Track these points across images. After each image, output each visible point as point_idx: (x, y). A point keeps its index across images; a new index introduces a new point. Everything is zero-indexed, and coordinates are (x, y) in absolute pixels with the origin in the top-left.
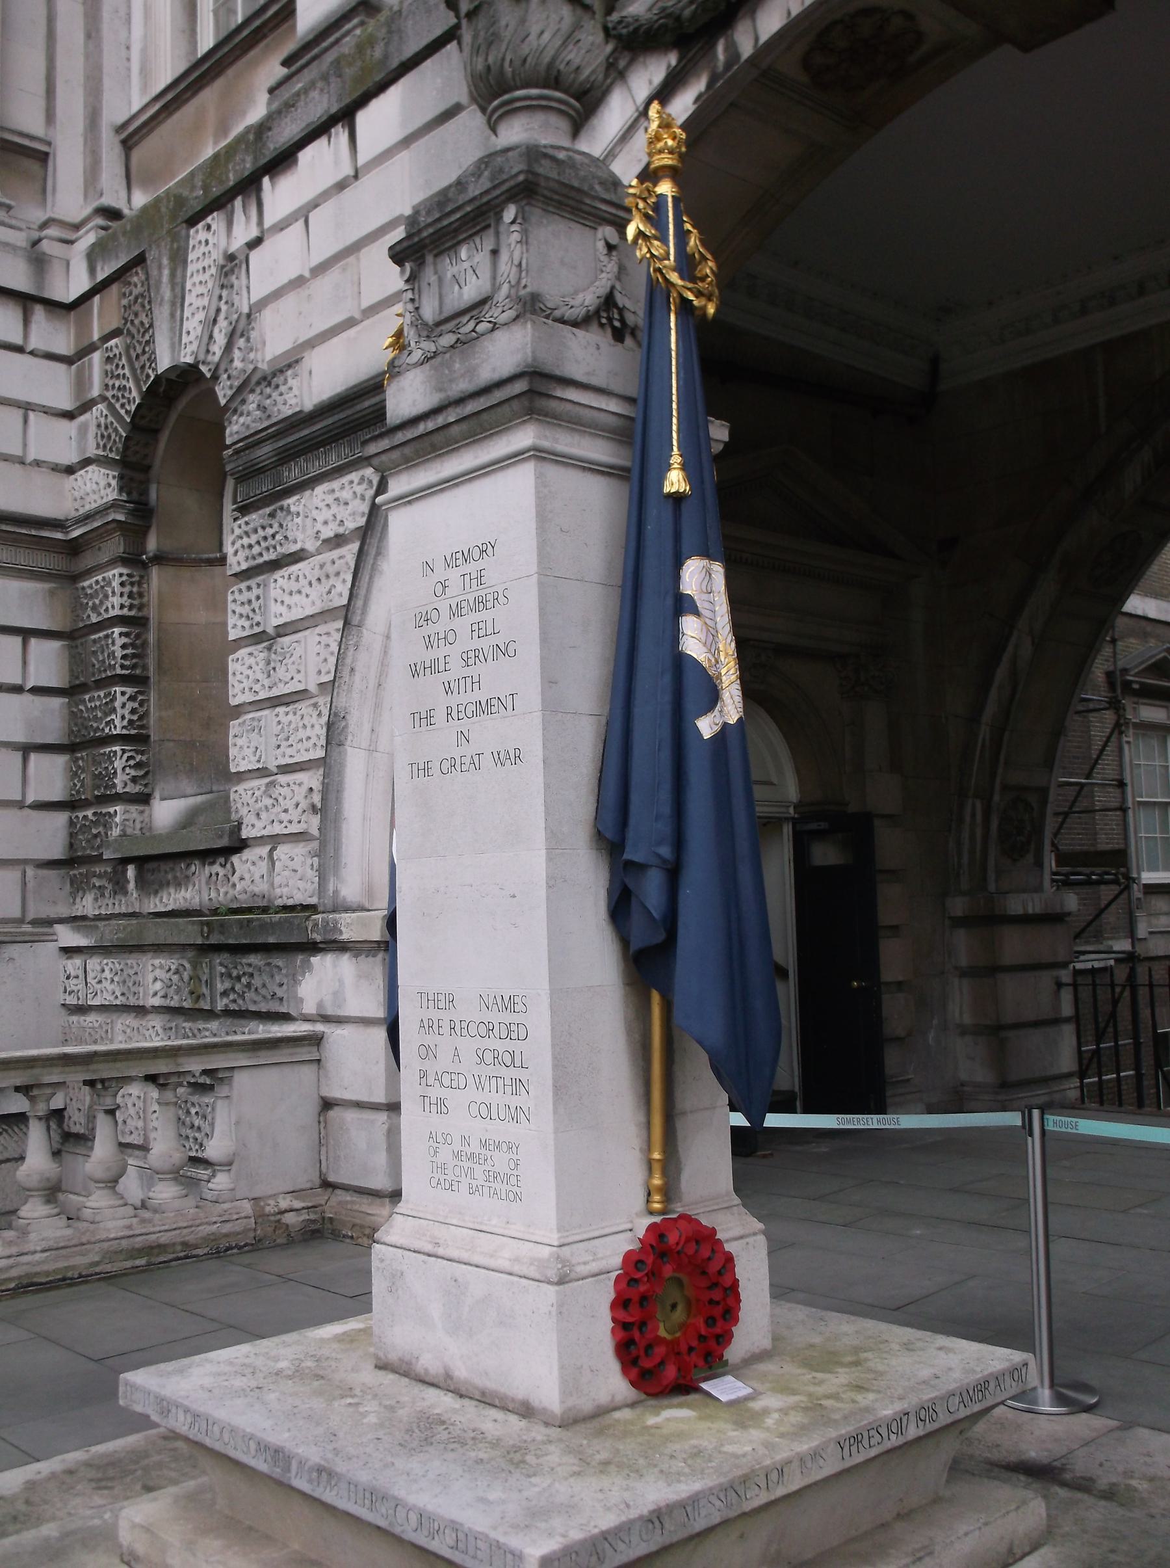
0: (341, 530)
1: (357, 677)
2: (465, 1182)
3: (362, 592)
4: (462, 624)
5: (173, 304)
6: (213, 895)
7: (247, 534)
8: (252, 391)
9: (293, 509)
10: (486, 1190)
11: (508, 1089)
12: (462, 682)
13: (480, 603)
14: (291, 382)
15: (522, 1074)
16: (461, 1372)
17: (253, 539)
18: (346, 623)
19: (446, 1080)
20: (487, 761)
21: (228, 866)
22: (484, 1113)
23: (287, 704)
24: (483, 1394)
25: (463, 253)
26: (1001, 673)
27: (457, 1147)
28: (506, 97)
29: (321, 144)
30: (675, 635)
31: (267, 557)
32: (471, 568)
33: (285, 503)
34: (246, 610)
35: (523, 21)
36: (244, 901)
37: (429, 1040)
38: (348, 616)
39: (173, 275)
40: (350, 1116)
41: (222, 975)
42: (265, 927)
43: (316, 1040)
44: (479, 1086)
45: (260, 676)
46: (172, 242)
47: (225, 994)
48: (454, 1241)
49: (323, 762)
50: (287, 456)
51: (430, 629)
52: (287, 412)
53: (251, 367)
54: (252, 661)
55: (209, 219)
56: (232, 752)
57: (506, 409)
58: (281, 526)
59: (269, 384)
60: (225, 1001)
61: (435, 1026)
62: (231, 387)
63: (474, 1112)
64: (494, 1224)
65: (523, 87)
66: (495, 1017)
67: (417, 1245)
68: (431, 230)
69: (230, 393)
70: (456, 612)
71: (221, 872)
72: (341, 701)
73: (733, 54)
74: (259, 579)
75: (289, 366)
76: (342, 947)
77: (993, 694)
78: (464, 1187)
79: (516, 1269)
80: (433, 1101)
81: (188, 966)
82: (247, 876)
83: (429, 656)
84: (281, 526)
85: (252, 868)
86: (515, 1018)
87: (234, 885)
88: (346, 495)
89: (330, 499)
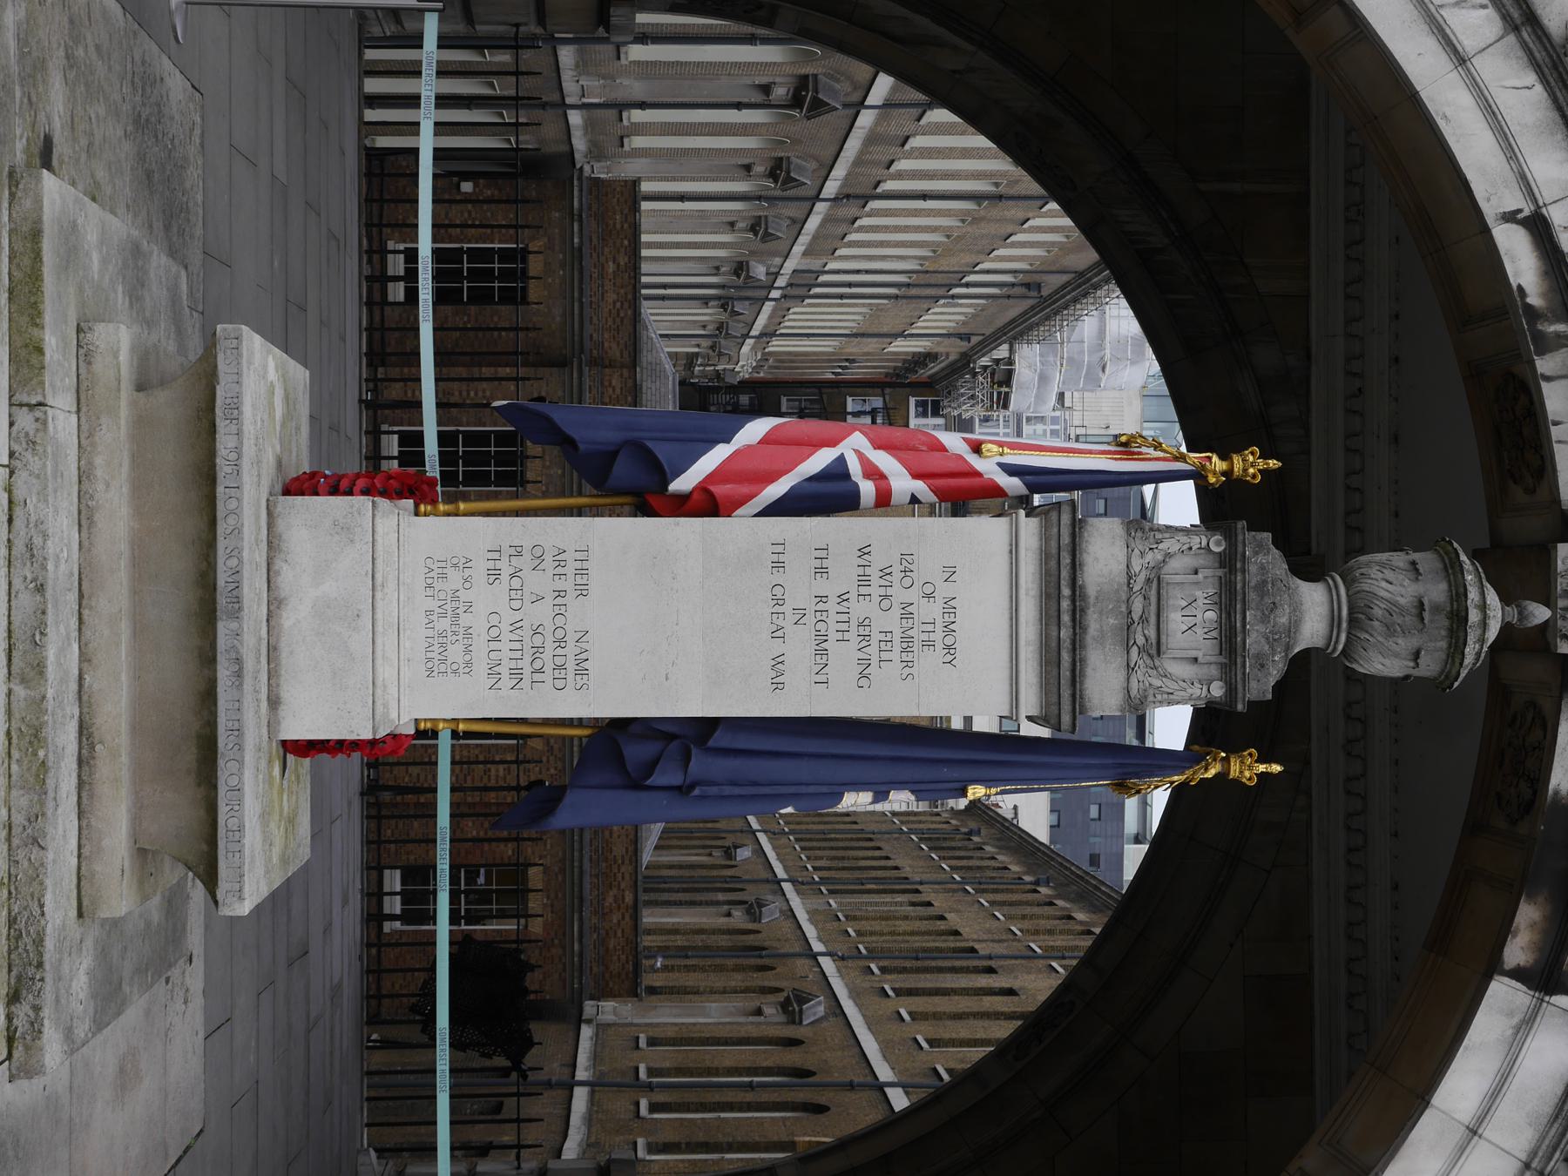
2: (432, 604)
4: (892, 622)
10: (430, 633)
11: (513, 664)
12: (844, 617)
13: (907, 640)
15: (526, 683)
19: (516, 583)
20: (777, 647)
22: (494, 632)
24: (275, 649)
25: (1211, 615)
28: (1344, 625)
30: (857, 786)
32: (938, 636)
35: (1397, 655)
37: (548, 558)
44: (516, 626)
51: (897, 575)
57: (1054, 699)
61: (560, 570)
63: (494, 620)
65: (1348, 638)
66: (571, 649)
67: (379, 562)
68: (1239, 586)
70: (907, 615)
78: (432, 604)
79: (379, 692)
80: (499, 565)
83: (874, 572)
86: (570, 676)
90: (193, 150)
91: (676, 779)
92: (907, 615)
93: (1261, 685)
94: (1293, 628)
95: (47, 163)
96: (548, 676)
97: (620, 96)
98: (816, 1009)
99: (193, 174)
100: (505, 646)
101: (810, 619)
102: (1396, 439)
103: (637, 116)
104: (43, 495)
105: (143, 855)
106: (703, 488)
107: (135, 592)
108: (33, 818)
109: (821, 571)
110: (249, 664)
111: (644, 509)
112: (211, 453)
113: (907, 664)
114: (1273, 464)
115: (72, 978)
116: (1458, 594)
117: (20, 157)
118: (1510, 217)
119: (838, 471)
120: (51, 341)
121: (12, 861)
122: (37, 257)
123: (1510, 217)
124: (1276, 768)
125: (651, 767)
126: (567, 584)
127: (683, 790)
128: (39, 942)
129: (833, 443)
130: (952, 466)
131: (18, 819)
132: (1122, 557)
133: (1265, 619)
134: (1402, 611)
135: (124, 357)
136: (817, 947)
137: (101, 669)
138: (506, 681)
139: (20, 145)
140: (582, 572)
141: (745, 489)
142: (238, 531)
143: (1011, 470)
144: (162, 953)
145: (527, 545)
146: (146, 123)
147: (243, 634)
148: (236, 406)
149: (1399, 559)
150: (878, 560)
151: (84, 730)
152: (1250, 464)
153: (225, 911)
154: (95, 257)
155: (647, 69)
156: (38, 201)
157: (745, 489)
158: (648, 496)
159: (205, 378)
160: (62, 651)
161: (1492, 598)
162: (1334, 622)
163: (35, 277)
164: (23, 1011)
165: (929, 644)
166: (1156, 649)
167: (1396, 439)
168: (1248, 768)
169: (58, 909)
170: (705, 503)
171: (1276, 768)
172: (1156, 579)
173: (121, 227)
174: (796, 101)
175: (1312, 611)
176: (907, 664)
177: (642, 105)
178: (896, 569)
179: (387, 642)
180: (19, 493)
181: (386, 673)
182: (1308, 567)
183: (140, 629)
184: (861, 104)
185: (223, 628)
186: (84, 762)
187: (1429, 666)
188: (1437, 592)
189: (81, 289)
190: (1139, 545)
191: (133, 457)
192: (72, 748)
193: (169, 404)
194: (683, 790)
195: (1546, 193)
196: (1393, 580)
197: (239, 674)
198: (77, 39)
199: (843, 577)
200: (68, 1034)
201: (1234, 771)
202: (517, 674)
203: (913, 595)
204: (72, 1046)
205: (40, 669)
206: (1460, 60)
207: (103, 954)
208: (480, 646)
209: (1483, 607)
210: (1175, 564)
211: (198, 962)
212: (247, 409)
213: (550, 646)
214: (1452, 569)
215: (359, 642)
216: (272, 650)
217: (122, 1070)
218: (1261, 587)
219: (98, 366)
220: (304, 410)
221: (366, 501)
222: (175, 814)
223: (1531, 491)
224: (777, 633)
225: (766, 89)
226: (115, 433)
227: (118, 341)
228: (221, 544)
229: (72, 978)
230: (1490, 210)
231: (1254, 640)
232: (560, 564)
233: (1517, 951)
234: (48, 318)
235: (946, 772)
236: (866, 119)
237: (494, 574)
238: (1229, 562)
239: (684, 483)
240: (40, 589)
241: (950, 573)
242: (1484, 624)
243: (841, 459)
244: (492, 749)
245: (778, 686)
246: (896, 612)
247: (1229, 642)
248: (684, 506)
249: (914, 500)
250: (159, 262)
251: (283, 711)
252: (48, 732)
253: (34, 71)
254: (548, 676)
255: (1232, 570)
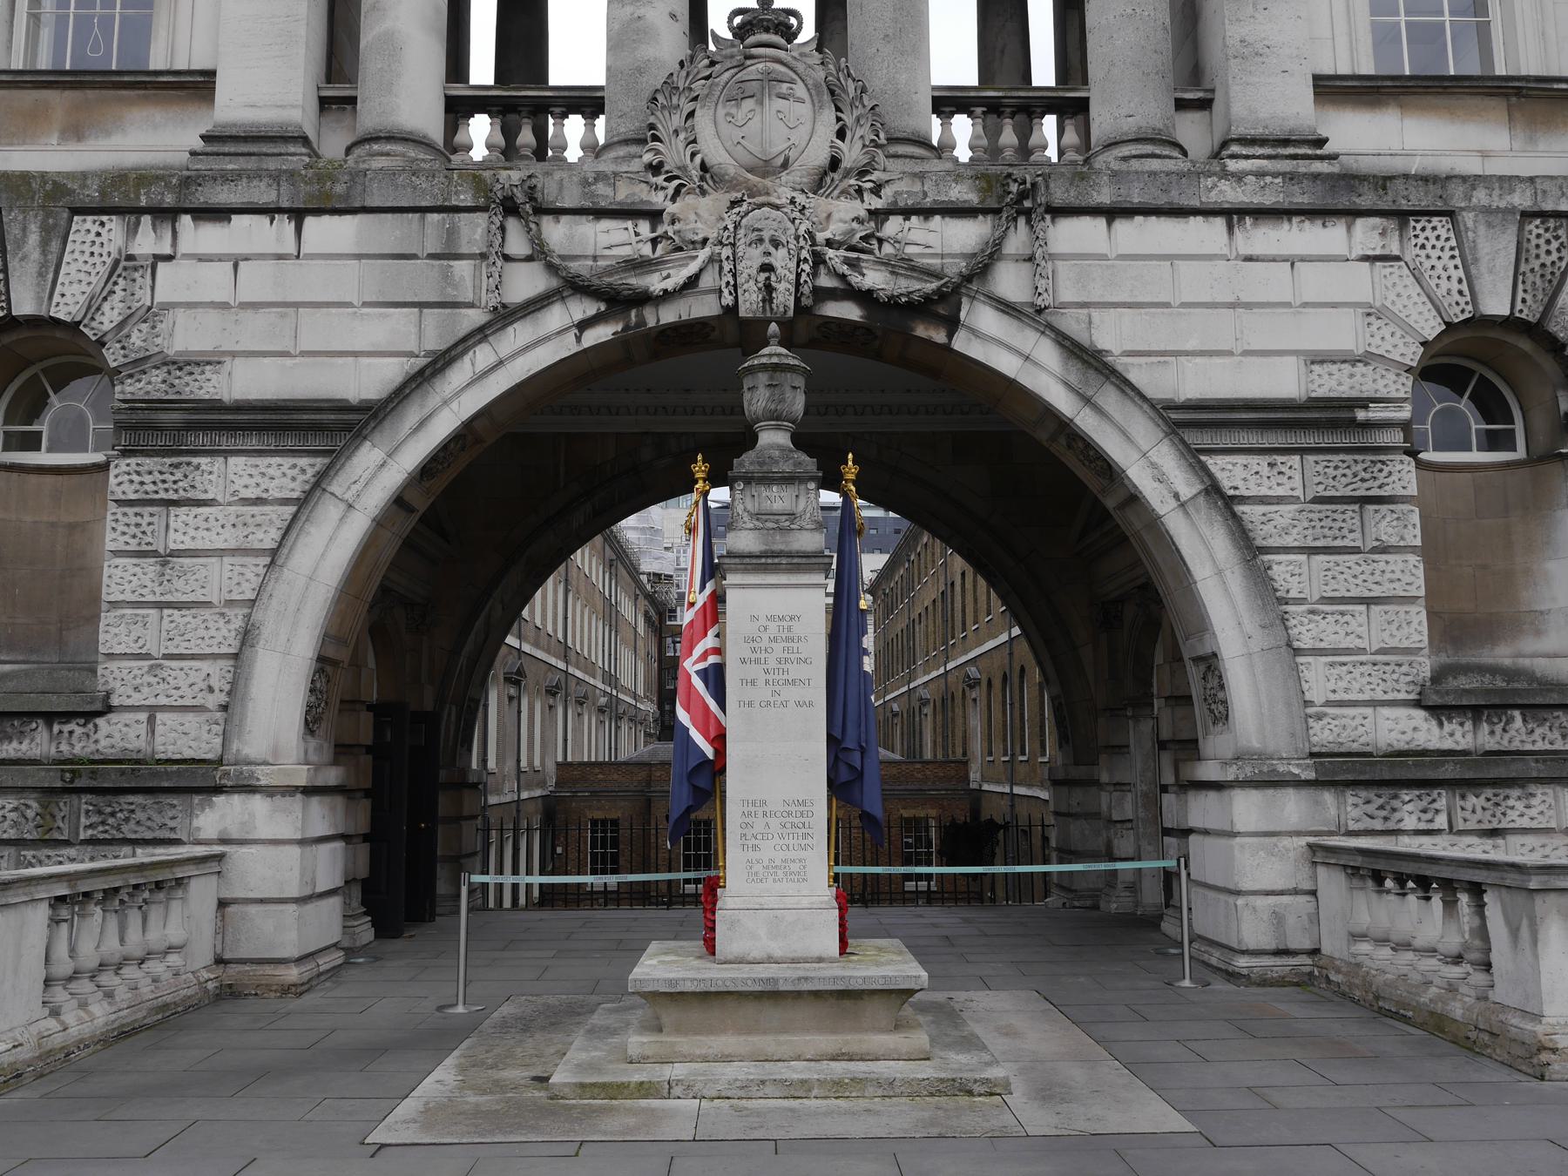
0: (264, 495)
1: (274, 602)
2: (770, 879)
3: (289, 544)
4: (778, 647)
5: (43, 265)
6: (64, 747)
7: (138, 473)
8: (157, 368)
9: (203, 467)
13: (787, 639)
14: (208, 375)
16: (778, 953)
17: (147, 479)
18: (272, 562)
20: (791, 704)
21: (91, 726)
23: (180, 609)
25: (775, 488)
26: (479, 624)
27: (766, 863)
29: (265, 220)
30: (861, 664)
31: (162, 495)
33: (195, 460)
34: (133, 530)
36: (111, 753)
38: (273, 555)
39: (44, 244)
40: (253, 909)
41: (87, 812)
42: (155, 774)
43: (220, 858)
44: (782, 837)
45: (149, 584)
46: (48, 216)
47: (91, 826)
48: (772, 902)
49: (236, 656)
50: (191, 427)
52: (202, 395)
53: (157, 350)
54: (137, 569)
55: (105, 218)
56: (102, 637)
58: (186, 476)
59: (180, 369)
60: (90, 832)
62: (125, 356)
64: (790, 892)
66: (793, 809)
69: (122, 360)
70: (775, 640)
71: (79, 731)
72: (257, 616)
73: (642, 322)
74: (151, 509)
75: (209, 363)
76: (248, 788)
77: (472, 636)
78: (770, 879)
81: (35, 805)
82: (117, 735)
83: (753, 656)
84: (186, 476)
85: (125, 729)
87: (96, 741)
88: (271, 471)
89: (253, 471)
90: (540, 1000)
91: (857, 755)
92: (775, 640)
93: (809, 463)
94: (781, 448)
95: (547, 1079)
96: (806, 820)
97: (514, 773)
98: (973, 671)
99: (552, 1000)
100: (791, 842)
101: (777, 688)
102: (688, 391)
103: (524, 763)
104: (716, 1081)
105: (898, 1027)
106: (711, 742)
107: (765, 1033)
108: (880, 1085)
109: (753, 682)
110: (801, 974)
111: (723, 770)
112: (694, 994)
113: (799, 639)
114: (700, 457)
115: (960, 1062)
116: (764, 368)
117: (543, 1094)
118: (578, 339)
119: (703, 674)
120: (637, 1078)
121: (901, 1095)
122: (593, 1085)
123: (578, 339)
124: (850, 456)
125: (851, 767)
126: (760, 811)
127: (863, 751)
128: (942, 1080)
129: (689, 677)
130: (701, 617)
131: (880, 1092)
132: (745, 533)
133: (777, 462)
134: (773, 394)
135: (645, 1040)
136: (942, 670)
137: (803, 1051)
138: (809, 841)
139: (537, 1094)
140: (754, 804)
141: (712, 721)
142: (733, 980)
143: (703, 587)
144: (947, 1015)
145: (740, 831)
146: (525, 1025)
147: (785, 977)
148: (670, 981)
149: (747, 396)
150: (747, 654)
151: (834, 1058)
152: (700, 468)
153: (926, 985)
154: (594, 1054)
155: (500, 759)
156: (565, 1085)
157: (712, 721)
158: (717, 768)
159: (654, 997)
160: (794, 1070)
161: (766, 351)
162: (778, 428)
163: (604, 1086)
164: (977, 1088)
165: (789, 628)
166: (792, 516)
167: (688, 391)
168: (851, 470)
169: (926, 1071)
170: (719, 740)
171: (850, 456)
172: (757, 516)
173: (579, 1040)
174: (517, 683)
175: (773, 439)
176: (799, 639)
177: (519, 761)
178: (752, 645)
179: (789, 902)
180: (715, 1094)
181: (805, 902)
182: (750, 440)
183: (784, 1031)
184: (519, 650)
185: (782, 987)
186: (851, 1058)
187: (800, 381)
188: (763, 378)
189: (610, 1062)
190: (740, 524)
191: (696, 1034)
192: (844, 1064)
193: (669, 1016)
194: (863, 751)
195: (567, 322)
196: (757, 400)
197: (806, 979)
198: (483, 1063)
199: (755, 671)
200: (988, 1064)
201: (852, 477)
202: (805, 836)
203: (765, 637)
204: (995, 1062)
205: (803, 1082)
206: (501, 363)
207: (948, 1046)
208: (791, 855)
209: (770, 355)
210: (749, 507)
211: (952, 994)
212: (672, 976)
213: (791, 819)
214: (752, 370)
215: (790, 916)
216: (793, 961)
217: (1007, 1034)
218: (761, 464)
219: (649, 1052)
220: (673, 944)
221: (718, 914)
222: (877, 1011)
223: (713, 329)
224: (784, 704)
225: (511, 698)
226: (684, 1043)
227: (637, 1042)
228: (740, 989)
229: (960, 1062)
230: (575, 349)
231: (787, 468)
232: (750, 814)
233: (939, 336)
234: (625, 1080)
235: (853, 619)
236: (526, 648)
237: (755, 848)
238: (748, 480)
239: (709, 752)
240: (763, 1082)
241: (754, 618)
242: (779, 355)
243: (697, 672)
244: (842, 849)
245: (811, 704)
246: (774, 645)
247: (788, 480)
248: (721, 751)
249: (717, 636)
250: (597, 1019)
251: (824, 955)
252: (835, 1077)
253: (499, 1086)
254: (806, 820)
255: (752, 478)
